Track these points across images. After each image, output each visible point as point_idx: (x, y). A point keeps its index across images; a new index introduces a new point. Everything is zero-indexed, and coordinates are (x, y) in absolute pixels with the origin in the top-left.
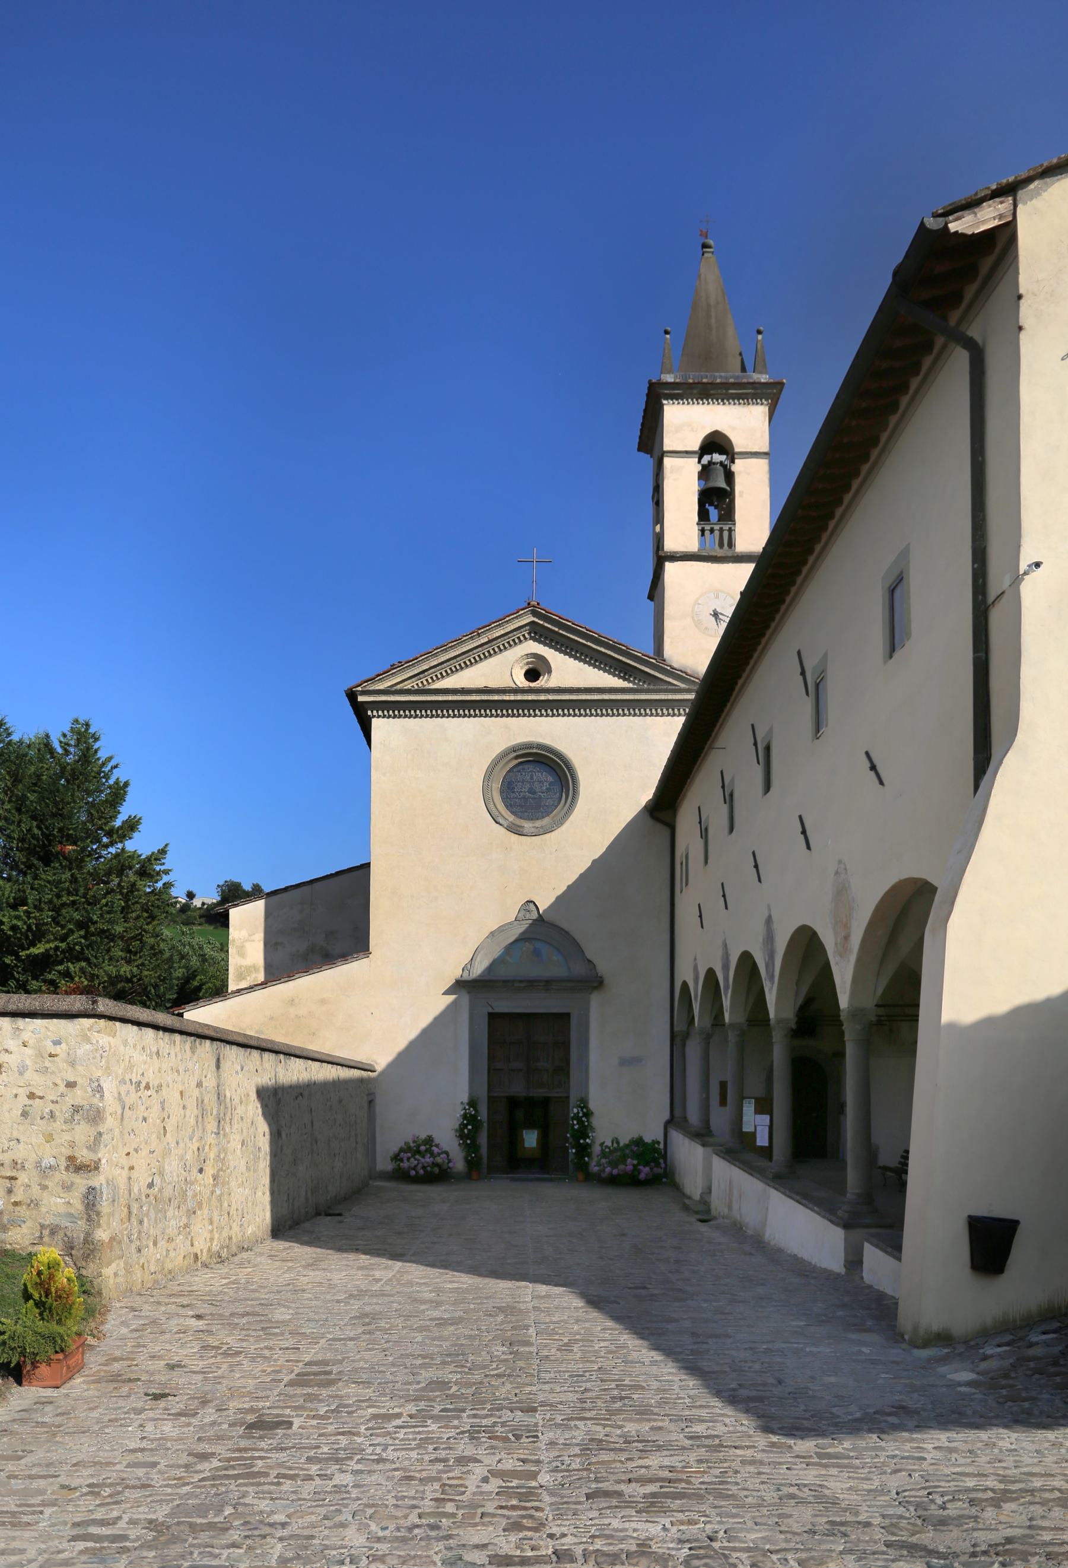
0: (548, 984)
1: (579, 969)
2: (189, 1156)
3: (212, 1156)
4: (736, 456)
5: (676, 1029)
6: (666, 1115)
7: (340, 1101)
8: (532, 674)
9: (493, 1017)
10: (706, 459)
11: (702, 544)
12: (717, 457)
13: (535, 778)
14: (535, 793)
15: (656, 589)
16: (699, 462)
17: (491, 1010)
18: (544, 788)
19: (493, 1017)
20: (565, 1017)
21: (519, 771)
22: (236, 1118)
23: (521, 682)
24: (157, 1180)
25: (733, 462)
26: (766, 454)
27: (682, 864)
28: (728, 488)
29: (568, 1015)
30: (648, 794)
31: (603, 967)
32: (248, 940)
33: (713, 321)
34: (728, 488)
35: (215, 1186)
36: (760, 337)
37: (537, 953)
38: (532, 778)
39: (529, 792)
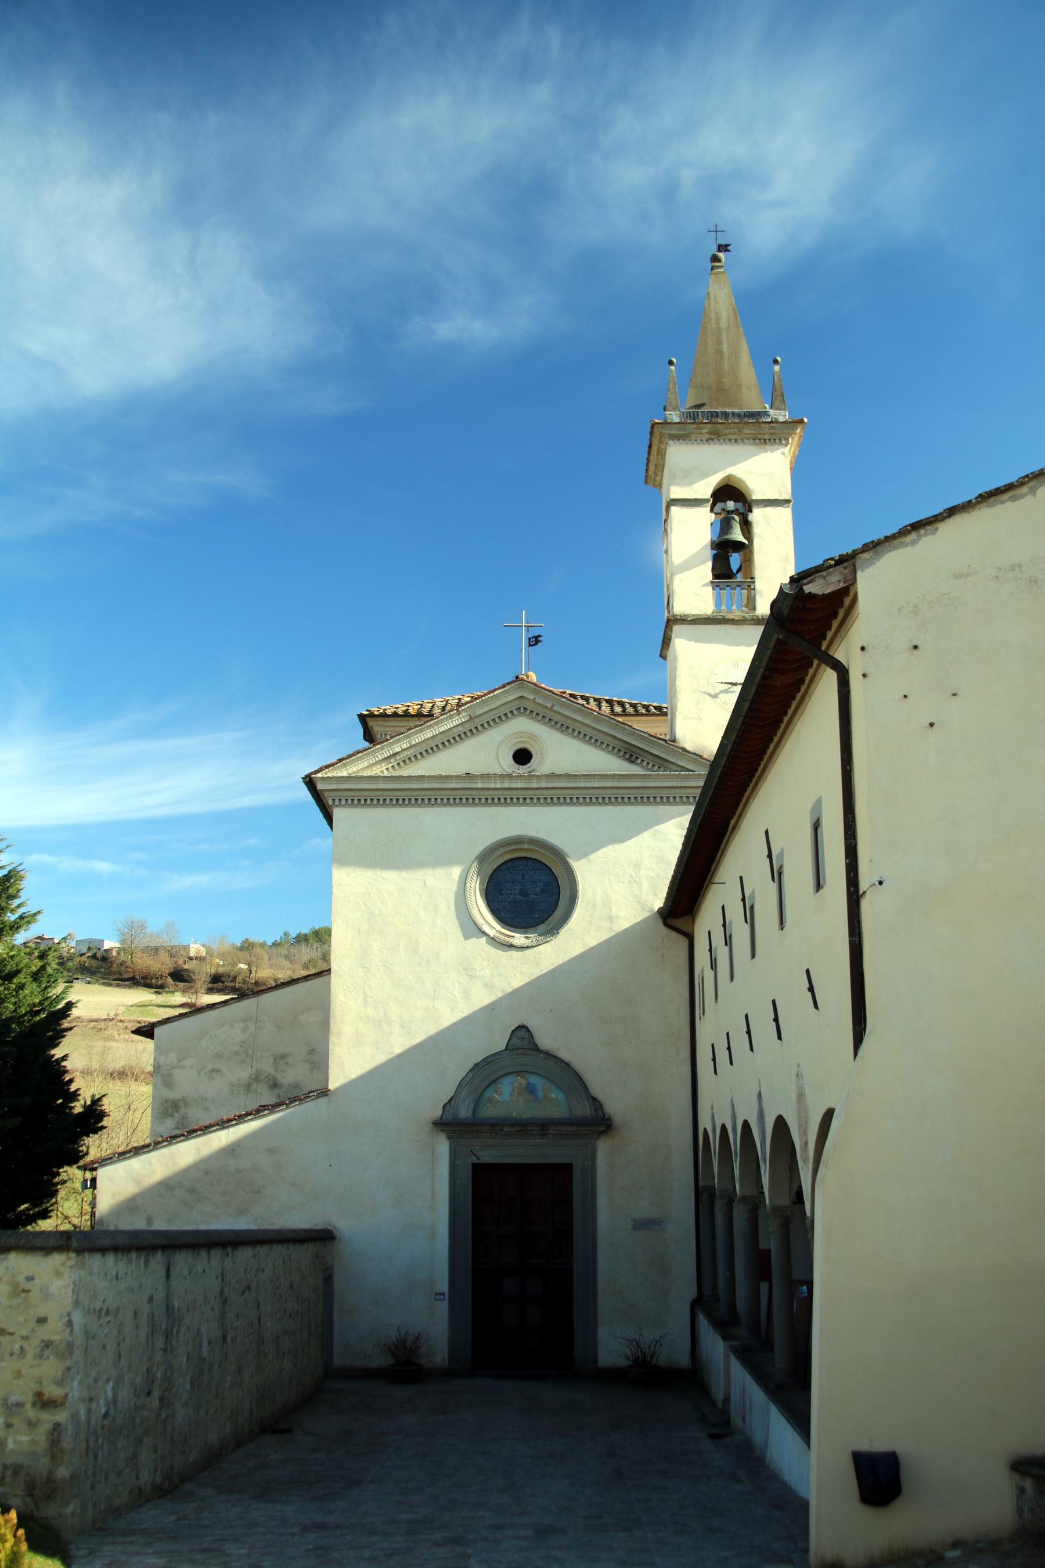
0: (544, 1127)
1: (584, 1110)
2: (138, 1380)
3: (159, 1375)
4: (753, 504)
5: (701, 1184)
6: (692, 1293)
7: (291, 1286)
8: (522, 757)
9: (479, 1169)
10: (719, 506)
11: (718, 602)
12: (731, 505)
13: (527, 877)
14: (526, 895)
15: (666, 641)
16: (712, 510)
17: (475, 1160)
18: (538, 889)
19: (479, 1169)
20: (566, 1169)
21: (508, 870)
22: (183, 1329)
23: (508, 764)
24: (112, 1410)
25: (750, 511)
26: (788, 501)
27: (699, 984)
28: (746, 542)
29: (569, 1167)
30: (658, 902)
31: (613, 1107)
32: (176, 1067)
33: (725, 347)
34: (746, 542)
35: (160, 1409)
36: (777, 368)
37: (531, 1089)
38: (523, 878)
39: (520, 894)
